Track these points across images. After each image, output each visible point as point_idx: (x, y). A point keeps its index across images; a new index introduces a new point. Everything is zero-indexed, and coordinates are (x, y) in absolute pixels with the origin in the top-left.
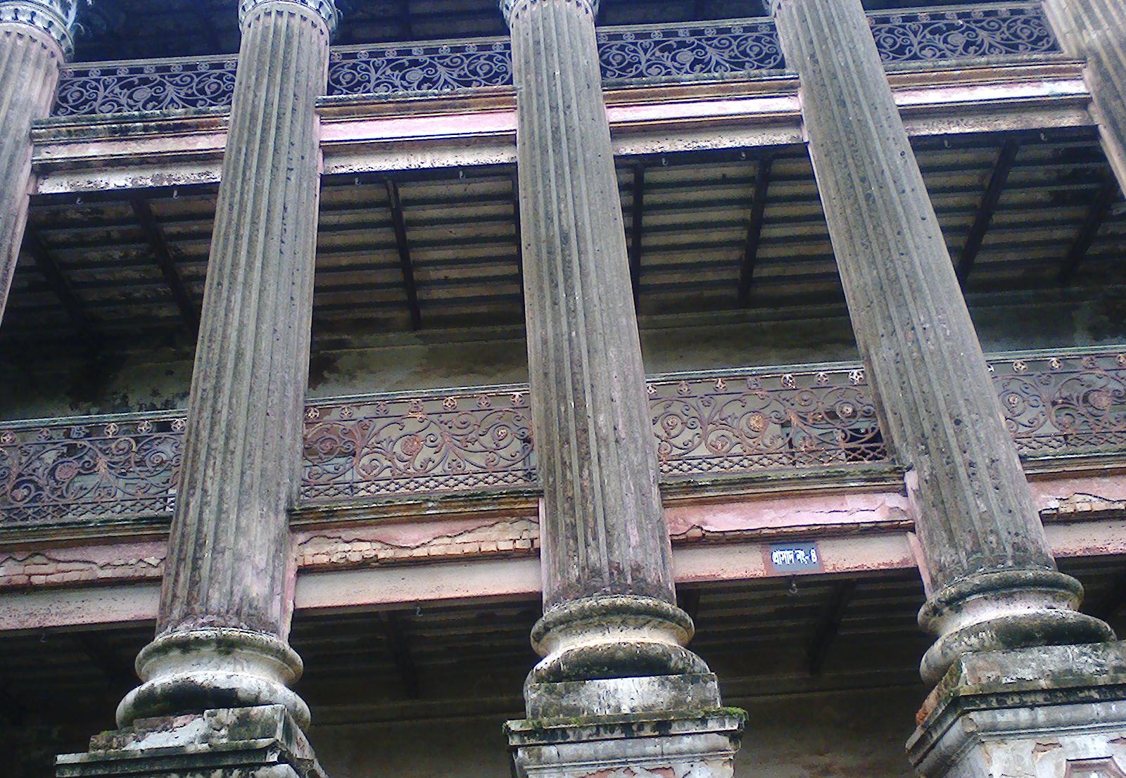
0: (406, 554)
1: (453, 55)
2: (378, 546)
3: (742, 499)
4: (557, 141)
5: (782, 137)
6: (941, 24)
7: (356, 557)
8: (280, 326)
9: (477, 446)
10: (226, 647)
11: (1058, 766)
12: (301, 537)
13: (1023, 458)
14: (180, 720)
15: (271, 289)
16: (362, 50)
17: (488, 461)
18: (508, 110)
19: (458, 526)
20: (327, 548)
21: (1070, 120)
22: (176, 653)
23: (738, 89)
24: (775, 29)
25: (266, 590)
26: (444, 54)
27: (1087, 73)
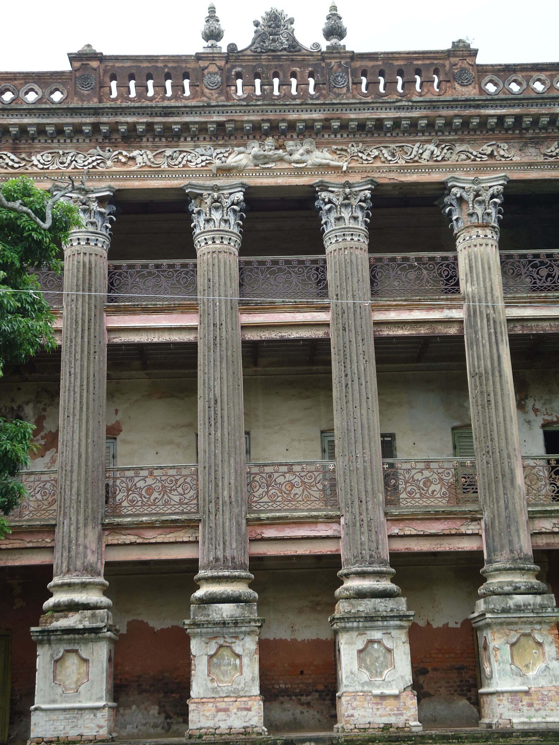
0: (147, 541)
2: (137, 537)
3: (278, 524)
4: (215, 344)
5: (319, 334)
6: (406, 264)
7: (128, 542)
8: (96, 439)
9: (176, 493)
10: (84, 586)
11: (363, 641)
12: (107, 533)
13: (386, 514)
14: (71, 614)
15: (91, 422)
16: (124, 263)
17: (180, 500)
18: (194, 313)
19: (168, 530)
20: (117, 538)
21: (453, 331)
22: (66, 588)
23: (302, 308)
25: (96, 560)
27: (465, 307)
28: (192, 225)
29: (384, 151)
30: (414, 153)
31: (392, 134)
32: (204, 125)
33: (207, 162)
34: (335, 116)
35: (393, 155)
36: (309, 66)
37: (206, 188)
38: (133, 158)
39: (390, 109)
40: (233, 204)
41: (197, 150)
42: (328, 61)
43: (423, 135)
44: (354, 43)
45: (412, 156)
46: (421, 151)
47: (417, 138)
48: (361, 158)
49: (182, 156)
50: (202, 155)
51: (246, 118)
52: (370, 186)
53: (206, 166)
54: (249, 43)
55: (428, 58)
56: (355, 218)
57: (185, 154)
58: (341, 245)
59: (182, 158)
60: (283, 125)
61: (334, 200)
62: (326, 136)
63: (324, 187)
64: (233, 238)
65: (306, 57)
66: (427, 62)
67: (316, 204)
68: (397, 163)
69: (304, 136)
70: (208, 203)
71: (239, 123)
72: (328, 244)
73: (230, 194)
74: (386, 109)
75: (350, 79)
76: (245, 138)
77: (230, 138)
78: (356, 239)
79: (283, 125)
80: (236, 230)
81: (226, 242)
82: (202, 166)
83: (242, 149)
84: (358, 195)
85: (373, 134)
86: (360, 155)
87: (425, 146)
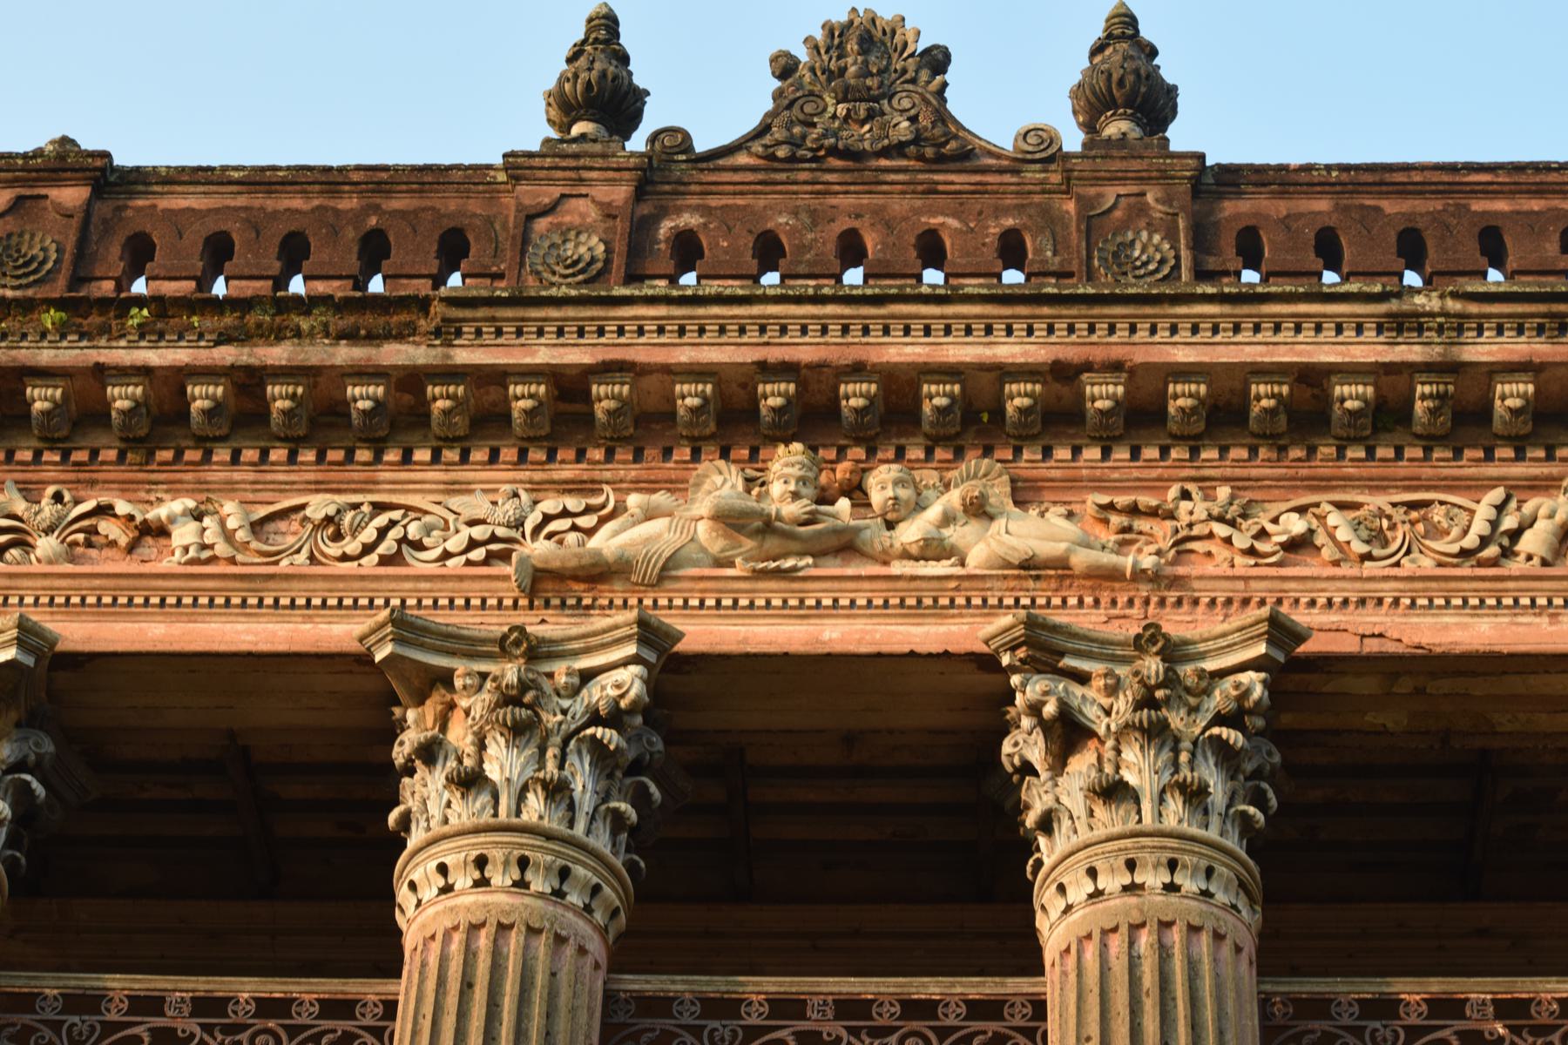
1: (259, 1023)
24: (1045, 1019)
26: (241, 1019)
28: (393, 817)
29: (1334, 518)
30: (1479, 527)
31: (1371, 452)
32: (493, 393)
33: (494, 547)
34: (1098, 355)
35: (1378, 537)
36: (999, 212)
37: (470, 647)
38: (160, 531)
39: (1359, 329)
40: (595, 719)
41: (455, 502)
42: (1092, 191)
43: (1520, 456)
44: (1204, 130)
45: (1471, 541)
46: (1509, 522)
47: (1491, 470)
48: (1228, 541)
49: (382, 520)
50: (472, 523)
51: (684, 356)
52: (1261, 648)
53: (486, 562)
54: (749, 122)
55: (1540, 191)
56: (1195, 796)
57: (396, 515)
58: (1119, 907)
59: (382, 533)
60: (855, 396)
61: (1092, 712)
62: (1063, 453)
63: (1044, 648)
64: (579, 871)
65: (989, 178)
66: (1536, 205)
67: (1007, 747)
68: (1397, 564)
69: (959, 453)
70: (477, 712)
71: (651, 382)
72: (1054, 914)
73: (587, 676)
74: (1339, 329)
75: (1185, 254)
76: (684, 453)
77: (610, 455)
78: (1189, 885)
79: (855, 396)
80: (601, 841)
81: (538, 884)
82: (469, 563)
83: (661, 498)
84: (1207, 692)
85: (1282, 449)
86: (1221, 530)
87: (1528, 508)
